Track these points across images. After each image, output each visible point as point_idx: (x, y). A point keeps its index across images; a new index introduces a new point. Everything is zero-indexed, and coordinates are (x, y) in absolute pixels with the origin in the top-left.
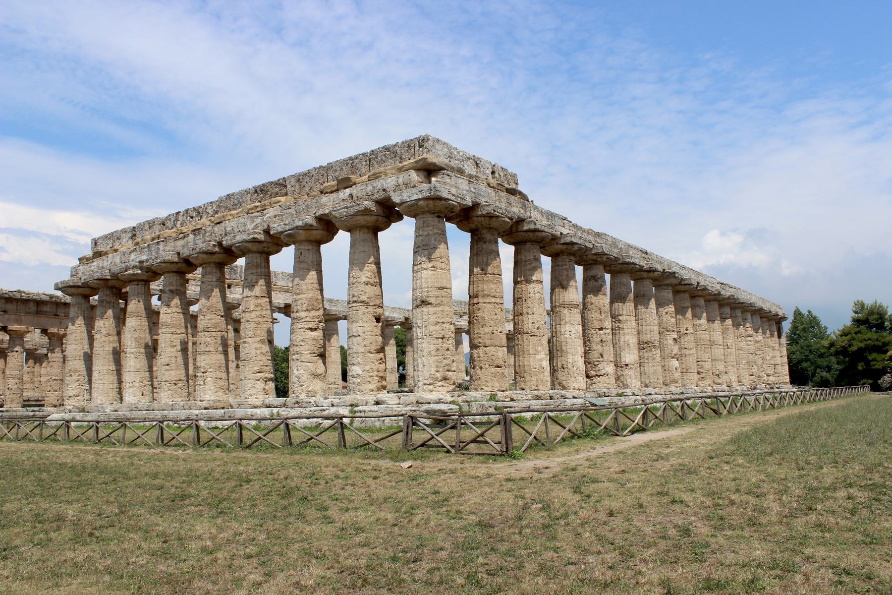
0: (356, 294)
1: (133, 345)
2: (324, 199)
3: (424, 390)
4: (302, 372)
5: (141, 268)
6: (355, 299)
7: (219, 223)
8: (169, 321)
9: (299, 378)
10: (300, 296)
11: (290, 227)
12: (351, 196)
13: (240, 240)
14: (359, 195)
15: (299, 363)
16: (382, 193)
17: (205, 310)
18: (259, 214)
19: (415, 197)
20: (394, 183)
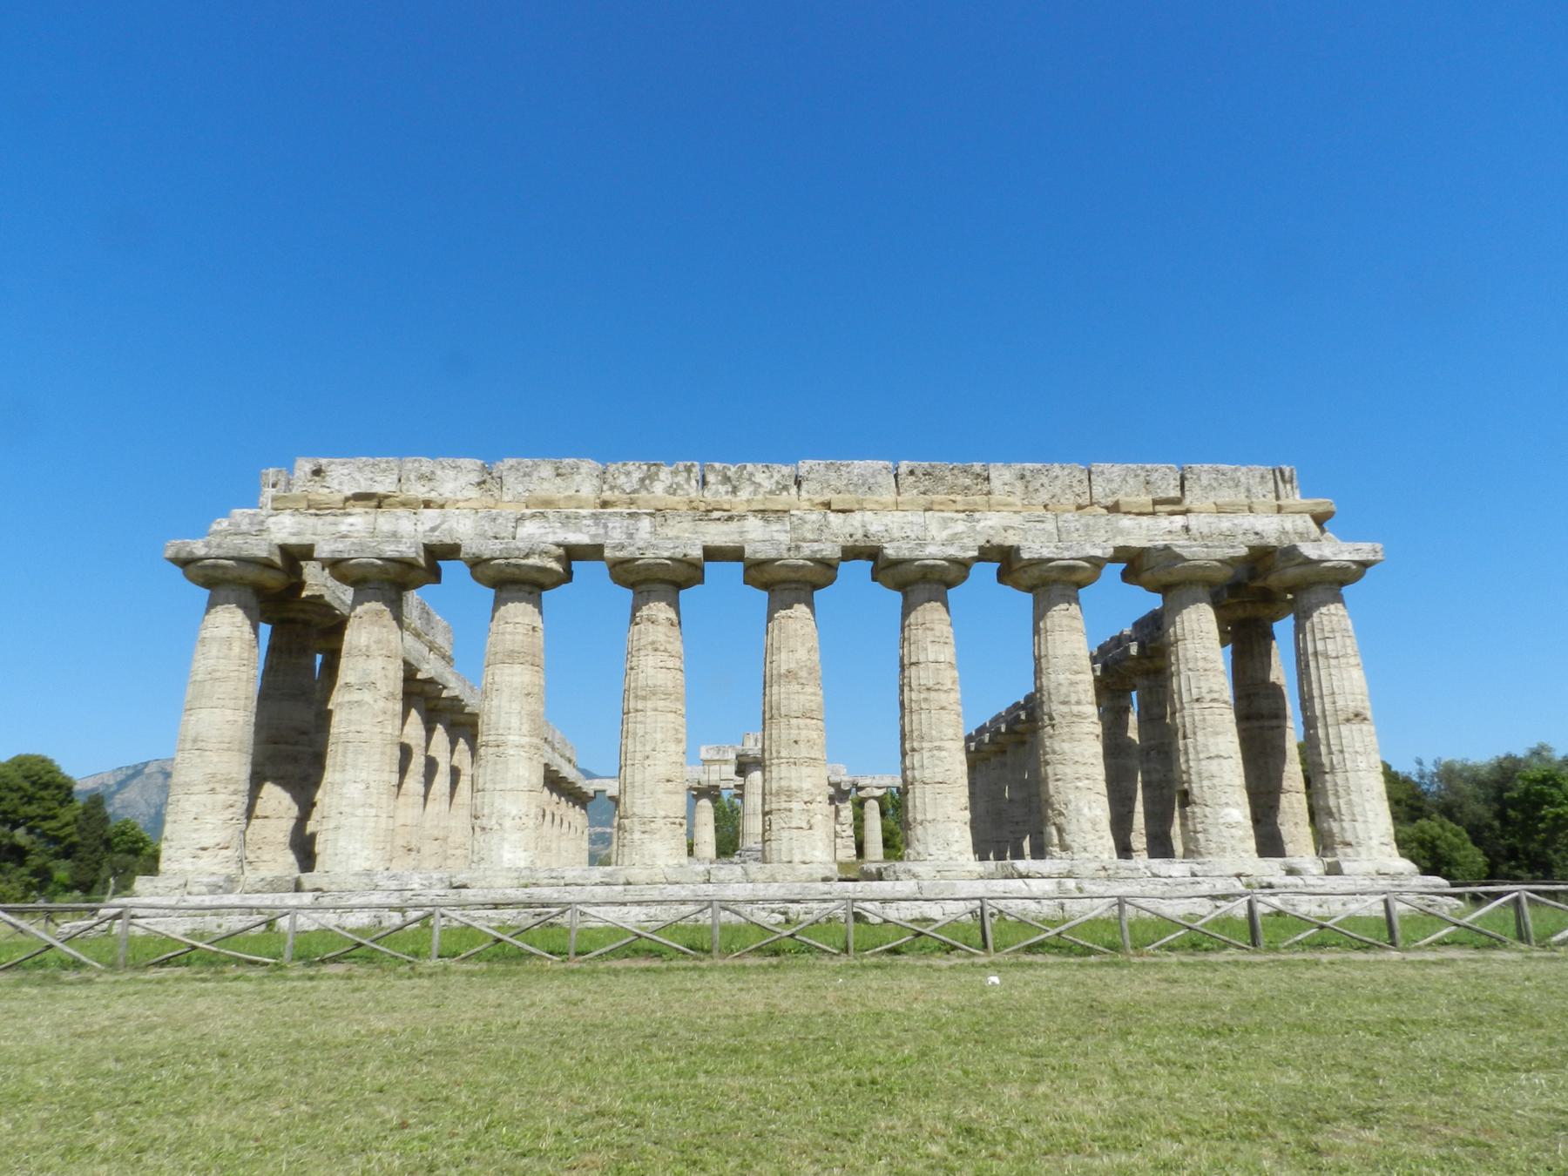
0: (1216, 688)
1: (526, 728)
2: (1126, 522)
3: (1382, 853)
4: (1098, 812)
5: (558, 559)
6: (1215, 696)
7: (843, 511)
8: (670, 684)
9: (1094, 824)
10: (1080, 677)
11: (1074, 555)
12: (1187, 529)
13: (940, 555)
14: (1205, 530)
15: (1093, 797)
16: (1252, 537)
17: (804, 674)
18: (962, 515)
19: (1347, 557)
20: (1274, 526)
